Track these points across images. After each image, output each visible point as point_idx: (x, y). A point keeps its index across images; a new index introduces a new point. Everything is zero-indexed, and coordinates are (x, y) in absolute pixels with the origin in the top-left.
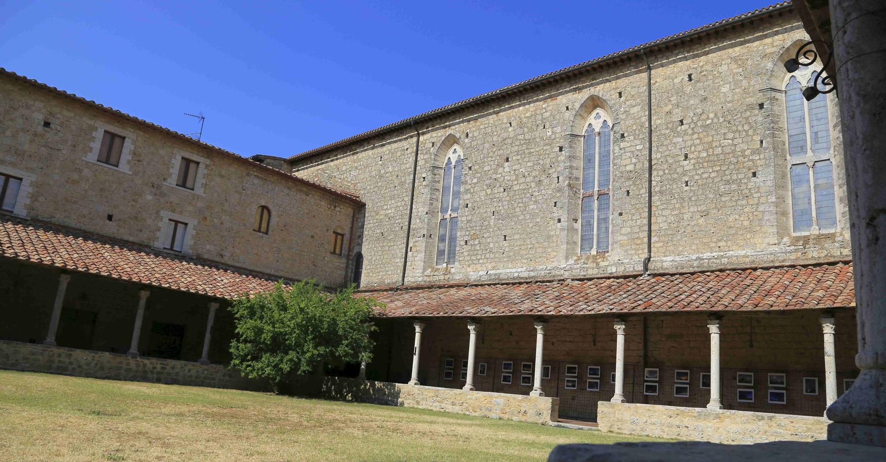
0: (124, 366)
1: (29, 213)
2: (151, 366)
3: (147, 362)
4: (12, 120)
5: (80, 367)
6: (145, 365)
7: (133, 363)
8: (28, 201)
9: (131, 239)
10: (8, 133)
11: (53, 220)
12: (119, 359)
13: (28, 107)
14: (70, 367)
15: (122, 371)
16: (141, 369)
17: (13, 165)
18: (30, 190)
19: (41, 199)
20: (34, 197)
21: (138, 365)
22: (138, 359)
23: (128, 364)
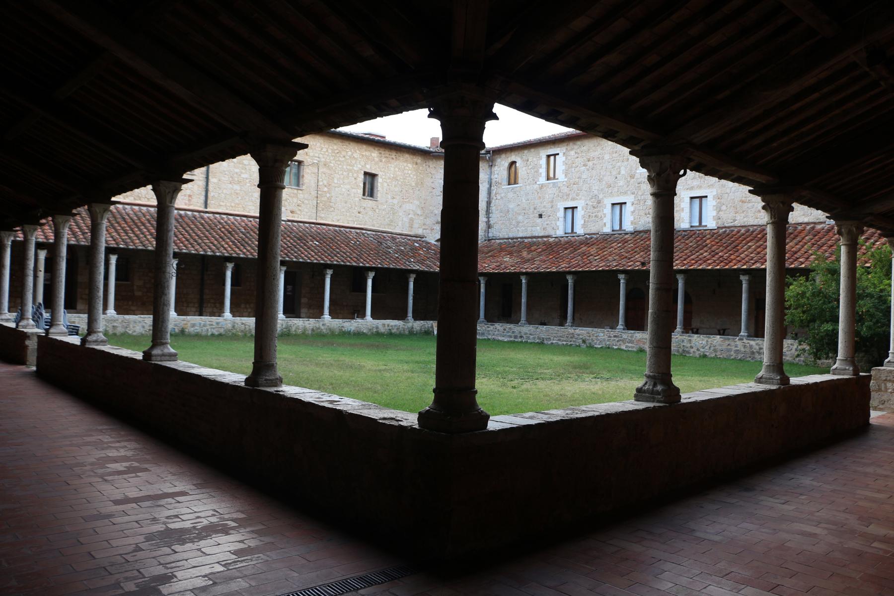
0: (734, 349)
1: (717, 223)
2: (758, 348)
3: (752, 343)
5: (698, 350)
6: (751, 347)
7: (739, 343)
8: (714, 213)
9: (806, 220)
11: (737, 223)
12: (727, 342)
14: (692, 350)
15: (732, 353)
16: (748, 350)
17: (700, 187)
18: (714, 203)
19: (724, 208)
20: (719, 209)
21: (745, 347)
22: (745, 341)
23: (736, 346)
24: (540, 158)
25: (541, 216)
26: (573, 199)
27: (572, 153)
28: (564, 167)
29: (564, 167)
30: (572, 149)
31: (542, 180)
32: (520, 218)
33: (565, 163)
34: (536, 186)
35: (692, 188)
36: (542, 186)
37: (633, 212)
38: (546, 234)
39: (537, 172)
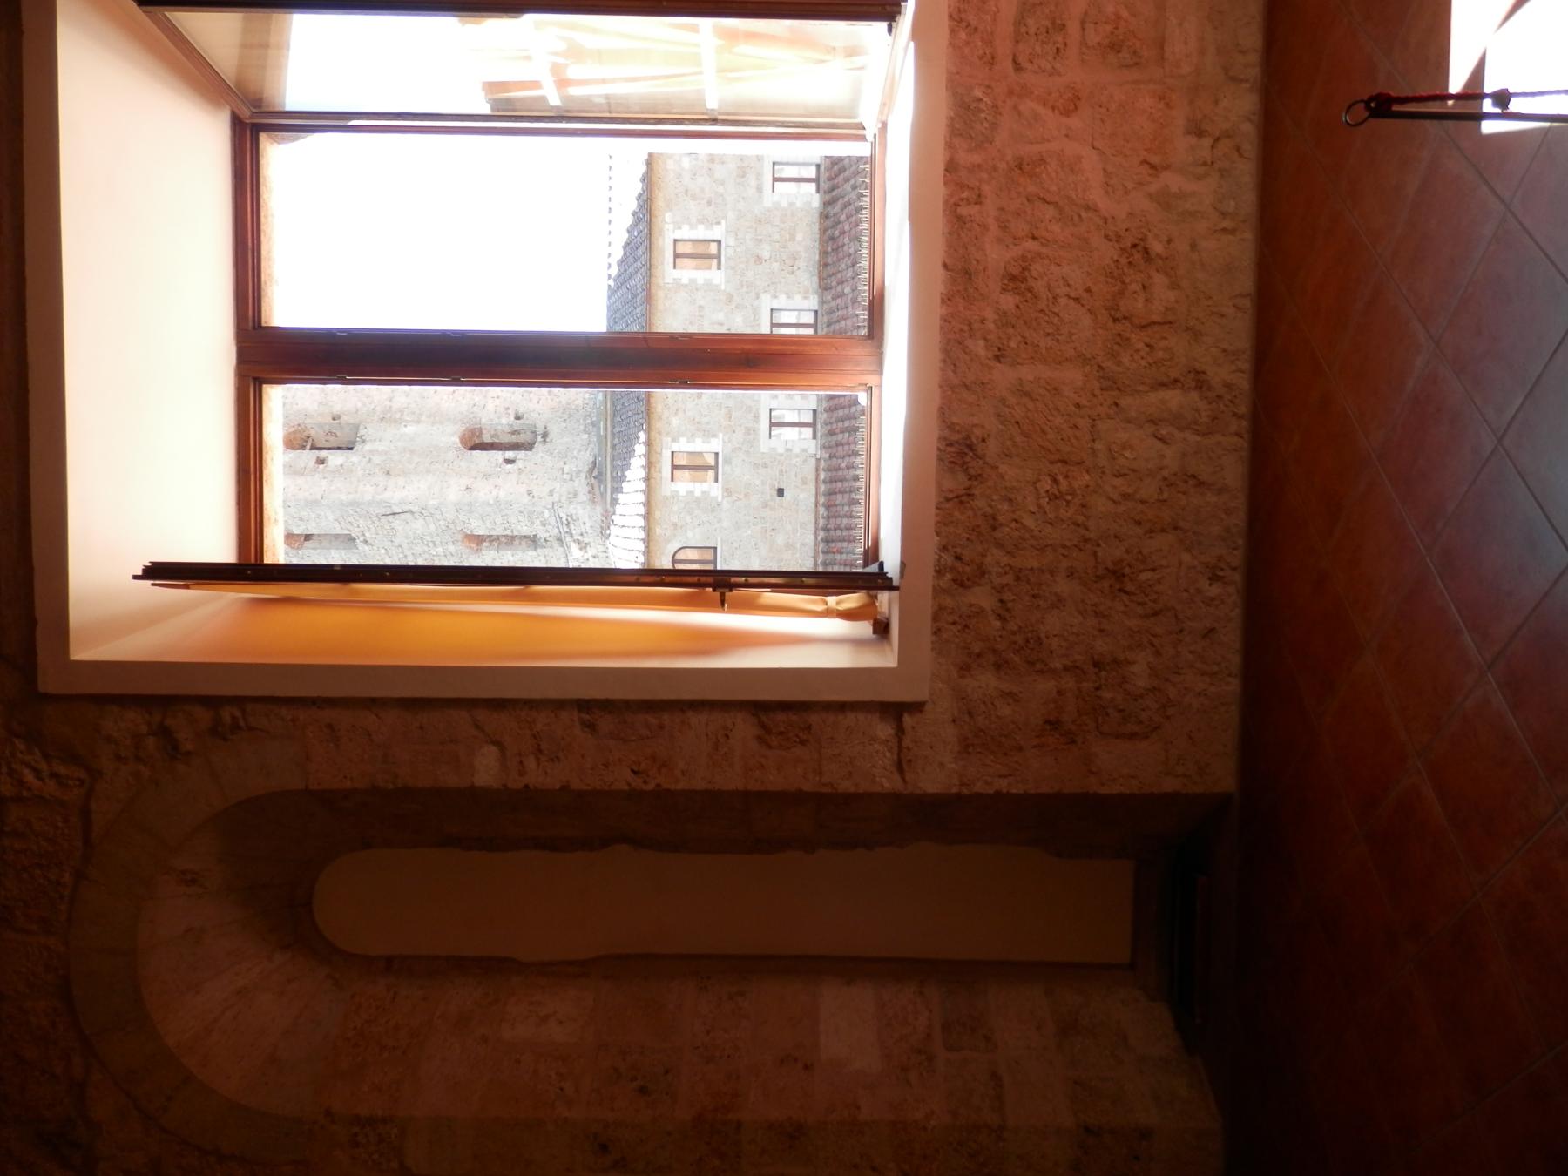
4: (702, 190)
10: (721, 189)
13: (679, 176)
17: (759, 176)
24: (675, 495)
25: (781, 492)
26: (757, 418)
27: (675, 421)
28: (699, 441)
29: (699, 441)
30: (669, 423)
31: (716, 490)
32: (780, 540)
33: (691, 438)
34: (726, 505)
35: (760, 189)
36: (728, 491)
37: (789, 297)
38: (812, 477)
39: (698, 501)
